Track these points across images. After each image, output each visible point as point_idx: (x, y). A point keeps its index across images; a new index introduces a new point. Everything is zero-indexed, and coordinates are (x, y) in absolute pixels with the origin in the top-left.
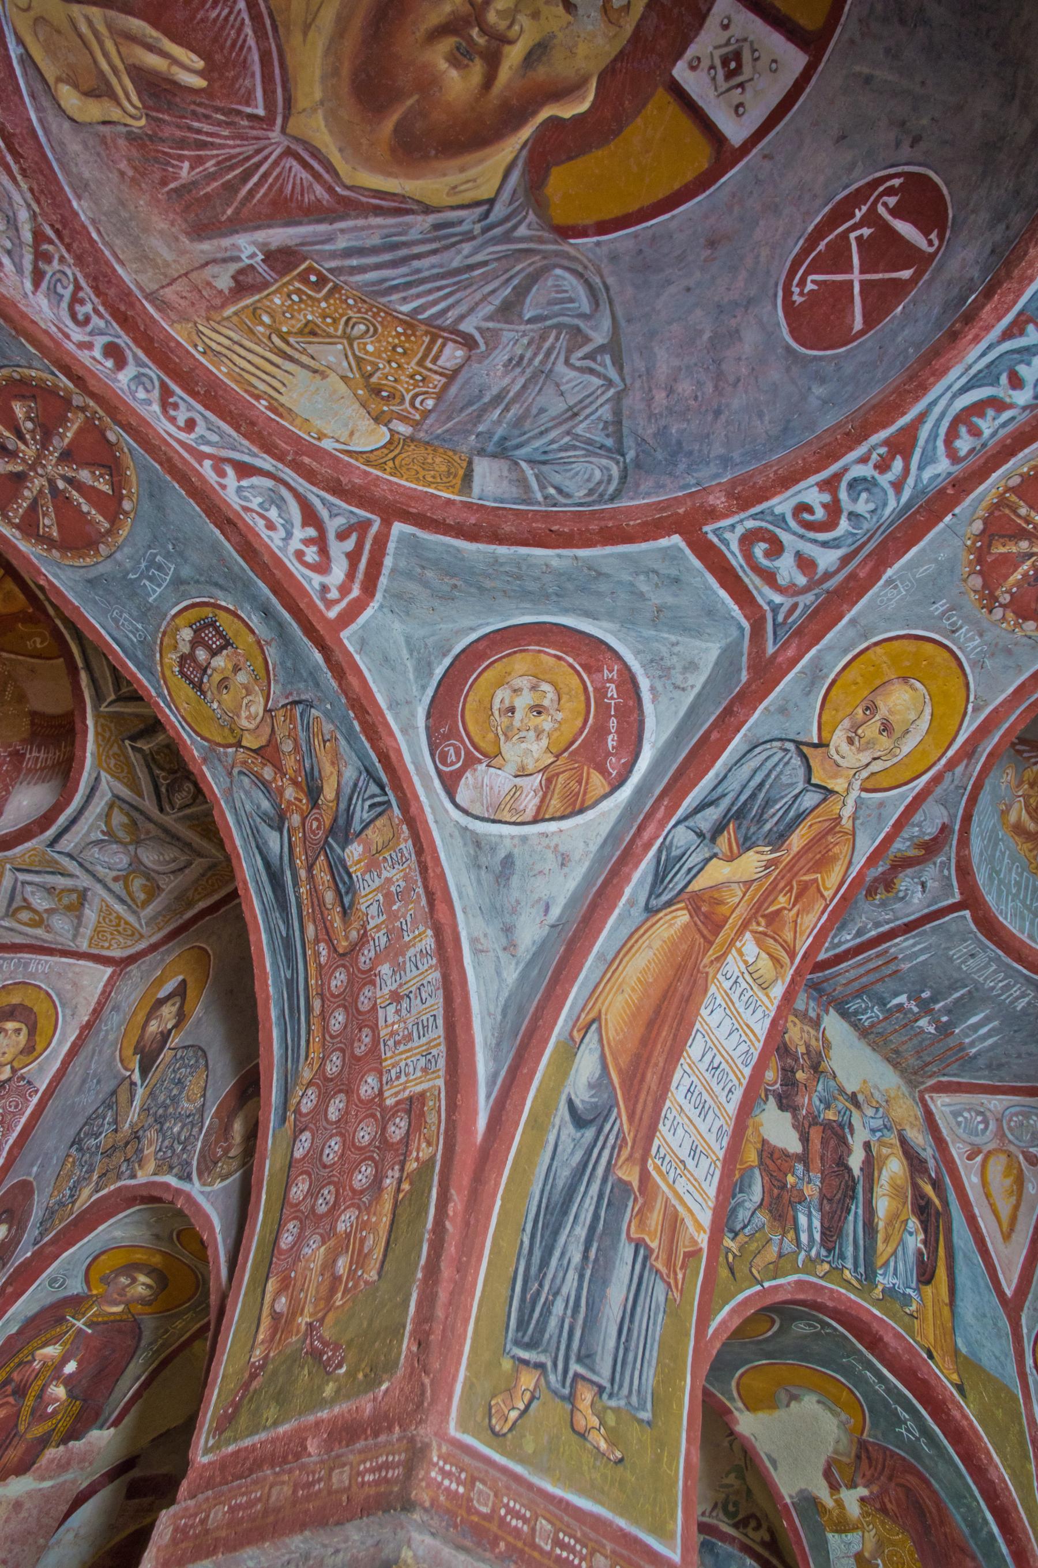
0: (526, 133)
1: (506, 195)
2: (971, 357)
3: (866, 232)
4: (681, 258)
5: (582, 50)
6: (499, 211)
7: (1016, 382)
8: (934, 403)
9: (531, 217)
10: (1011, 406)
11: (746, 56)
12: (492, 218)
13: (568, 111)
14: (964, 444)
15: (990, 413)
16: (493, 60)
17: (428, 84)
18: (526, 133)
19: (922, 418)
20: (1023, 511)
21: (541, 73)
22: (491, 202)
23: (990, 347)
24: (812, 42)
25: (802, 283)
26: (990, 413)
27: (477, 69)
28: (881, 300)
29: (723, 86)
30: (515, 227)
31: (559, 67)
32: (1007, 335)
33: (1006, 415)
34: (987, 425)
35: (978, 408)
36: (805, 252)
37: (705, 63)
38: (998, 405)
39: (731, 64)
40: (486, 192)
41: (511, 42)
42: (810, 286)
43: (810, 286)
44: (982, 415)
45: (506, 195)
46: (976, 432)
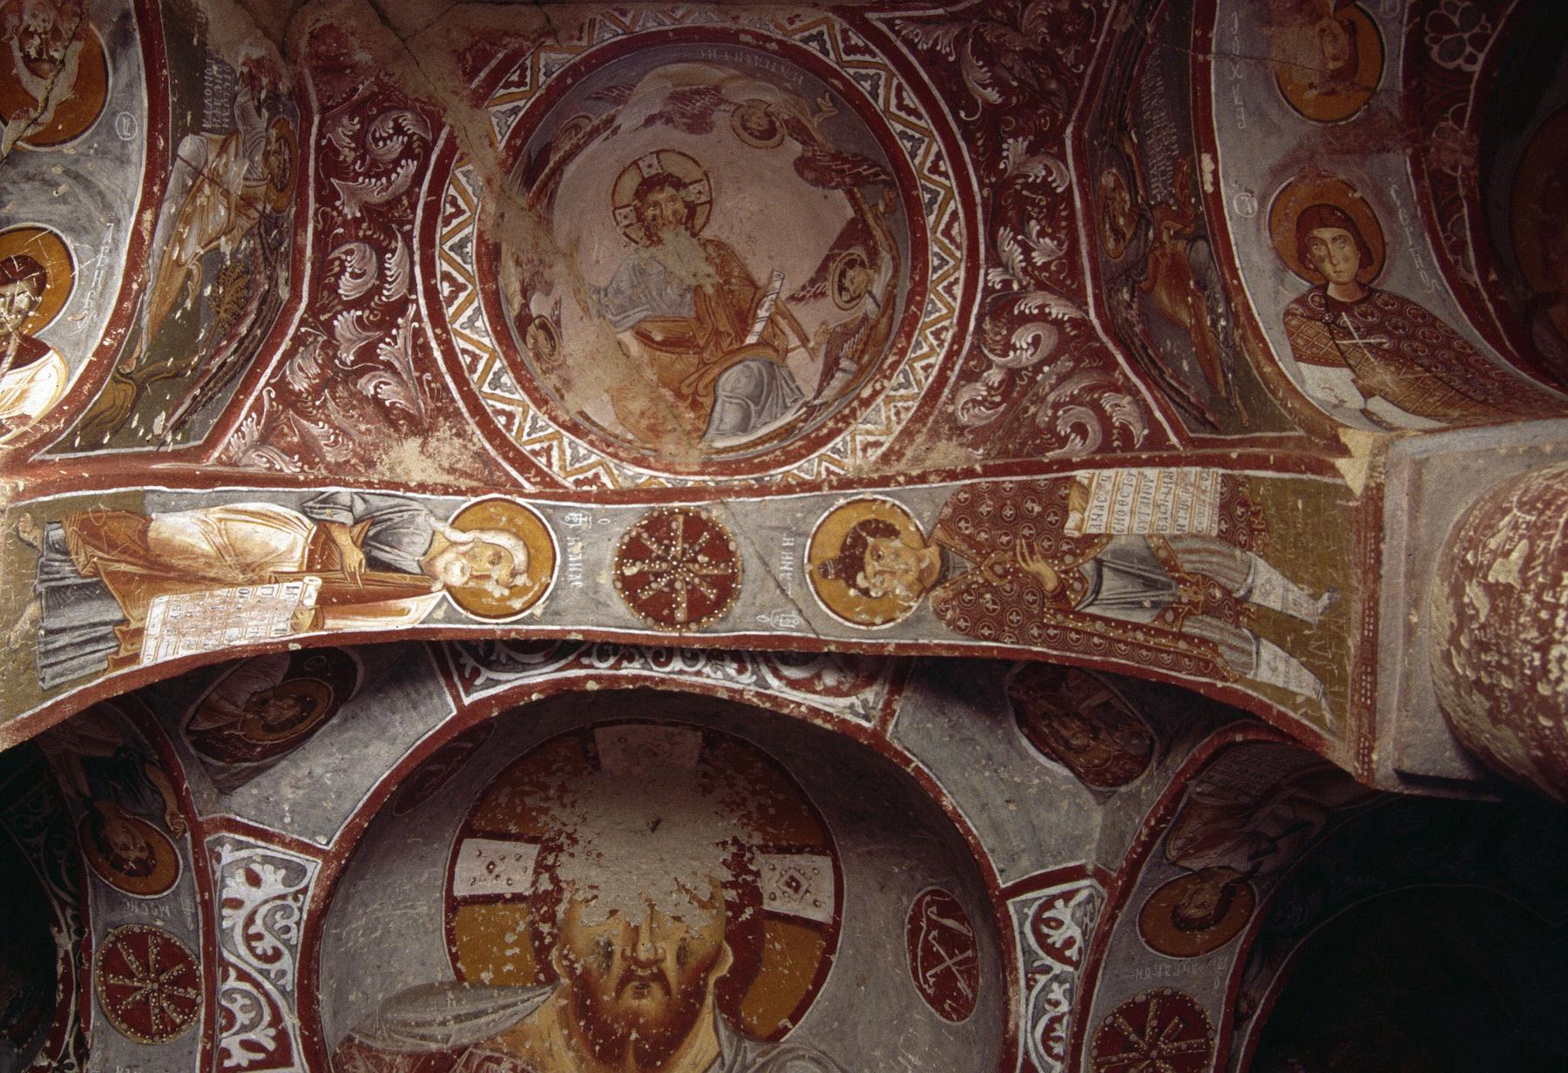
0: (710, 1000)
1: (725, 1044)
2: (1022, 1009)
3: (935, 933)
4: (851, 1006)
5: (706, 934)
6: (728, 1054)
7: (1056, 1004)
8: (1026, 1043)
9: (747, 1044)
10: (1063, 1015)
11: (797, 876)
12: (727, 1062)
13: (723, 970)
14: (1058, 1049)
15: (1057, 1026)
16: (660, 977)
17: (633, 1019)
18: (710, 1000)
19: (1026, 1053)
20: (1114, 1059)
21: (692, 962)
22: (720, 1054)
23: (1027, 1000)
24: (825, 847)
25: (926, 981)
26: (1057, 1026)
27: (656, 988)
28: (970, 972)
29: (798, 896)
30: (744, 1057)
31: (700, 950)
32: (1029, 988)
33: (1065, 1021)
34: (1061, 1031)
35: (1049, 1028)
36: (914, 959)
37: (779, 893)
38: (1058, 1019)
39: (794, 884)
40: (713, 1052)
41: (663, 960)
42: (931, 980)
43: (931, 980)
44: (1054, 1030)
45: (725, 1044)
46: (1059, 1039)
